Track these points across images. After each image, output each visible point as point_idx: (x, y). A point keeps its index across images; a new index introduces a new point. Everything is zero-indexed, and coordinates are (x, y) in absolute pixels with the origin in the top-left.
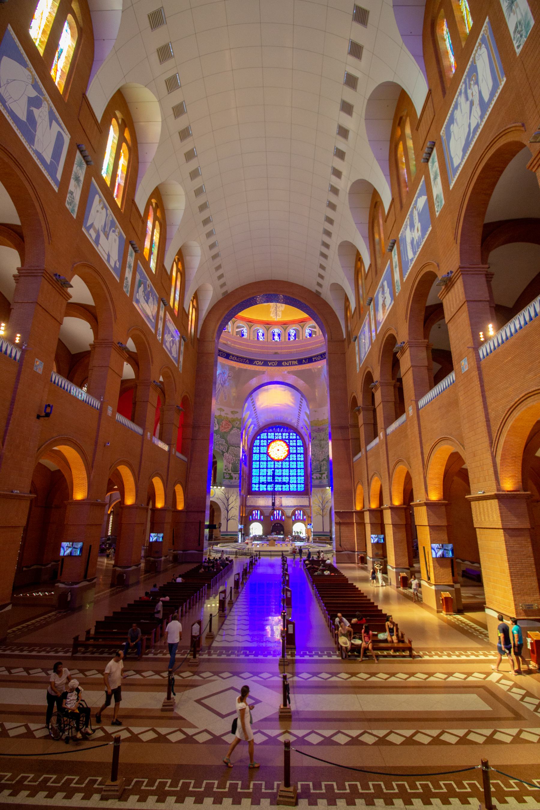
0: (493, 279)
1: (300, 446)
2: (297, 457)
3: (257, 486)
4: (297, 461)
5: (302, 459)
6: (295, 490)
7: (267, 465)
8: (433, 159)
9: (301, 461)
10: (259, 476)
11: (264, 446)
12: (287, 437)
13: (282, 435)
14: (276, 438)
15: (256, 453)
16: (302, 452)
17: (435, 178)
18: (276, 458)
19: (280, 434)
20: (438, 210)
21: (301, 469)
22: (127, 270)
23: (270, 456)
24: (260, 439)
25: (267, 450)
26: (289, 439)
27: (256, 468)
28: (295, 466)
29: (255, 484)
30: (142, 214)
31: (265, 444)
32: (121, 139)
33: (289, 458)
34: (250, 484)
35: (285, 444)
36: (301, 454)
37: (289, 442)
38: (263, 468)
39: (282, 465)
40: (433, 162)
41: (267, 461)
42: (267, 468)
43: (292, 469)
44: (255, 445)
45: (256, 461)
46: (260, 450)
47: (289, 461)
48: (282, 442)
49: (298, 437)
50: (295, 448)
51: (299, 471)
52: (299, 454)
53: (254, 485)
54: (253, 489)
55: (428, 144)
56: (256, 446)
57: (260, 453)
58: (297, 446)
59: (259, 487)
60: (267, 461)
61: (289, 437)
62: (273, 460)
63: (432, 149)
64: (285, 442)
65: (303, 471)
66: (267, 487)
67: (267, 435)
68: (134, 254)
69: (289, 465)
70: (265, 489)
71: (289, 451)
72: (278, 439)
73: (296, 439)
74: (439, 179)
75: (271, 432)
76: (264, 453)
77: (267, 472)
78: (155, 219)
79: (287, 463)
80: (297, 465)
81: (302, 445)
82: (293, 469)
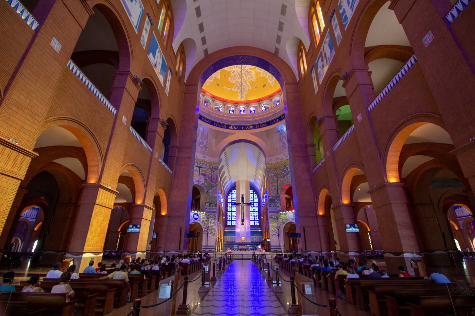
0: (372, 75)
8: (334, 18)
17: (336, 27)
20: (338, 43)
22: (167, 82)
29: (229, 221)
30: (175, 54)
32: (167, 15)
34: (226, 220)
40: (334, 20)
44: (229, 197)
49: (254, 193)
53: (228, 222)
55: (332, 11)
63: (333, 14)
65: (257, 213)
68: (171, 75)
74: (338, 28)
78: (181, 58)
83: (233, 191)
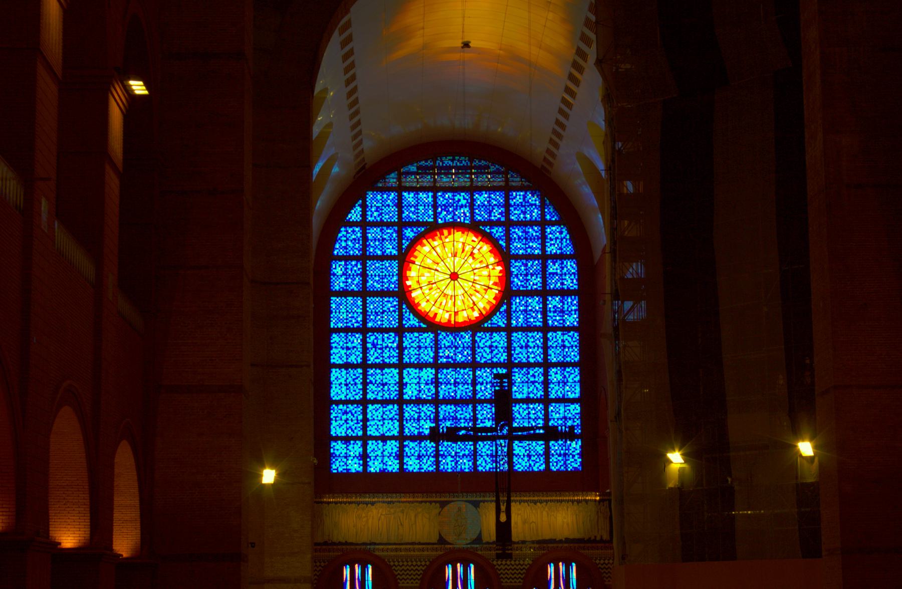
1: (560, 257)
2: (544, 312)
3: (356, 448)
4: (545, 329)
5: (572, 320)
6: (539, 466)
7: (401, 348)
9: (565, 329)
10: (364, 402)
11: (383, 258)
12: (496, 215)
13: (472, 205)
14: (444, 217)
15: (344, 293)
16: (570, 282)
18: (443, 317)
19: (462, 198)
21: (563, 365)
23: (414, 308)
24: (364, 225)
25: (402, 276)
26: (508, 224)
27: (347, 366)
28: (536, 355)
29: (347, 440)
31: (391, 249)
33: (509, 314)
35: (486, 248)
36: (564, 293)
37: (509, 240)
38: (382, 366)
39: (473, 347)
41: (400, 331)
42: (401, 366)
43: (521, 365)
45: (347, 330)
46: (364, 275)
47: (509, 330)
48: (470, 239)
50: (535, 265)
51: (555, 375)
52: (555, 293)
53: (338, 448)
54: (337, 466)
56: (347, 258)
57: (364, 293)
58: (544, 258)
59: (364, 457)
60: (400, 331)
61: (507, 213)
62: (430, 325)
64: (487, 238)
65: (574, 375)
66: (400, 456)
67: (399, 205)
69: (509, 349)
70: (393, 466)
71: (506, 279)
72: (455, 226)
73: (543, 223)
75: (416, 190)
76: (383, 294)
77: (402, 385)
79: (499, 339)
80: (546, 348)
81: (569, 250)
82: (529, 365)
83: (374, 199)
